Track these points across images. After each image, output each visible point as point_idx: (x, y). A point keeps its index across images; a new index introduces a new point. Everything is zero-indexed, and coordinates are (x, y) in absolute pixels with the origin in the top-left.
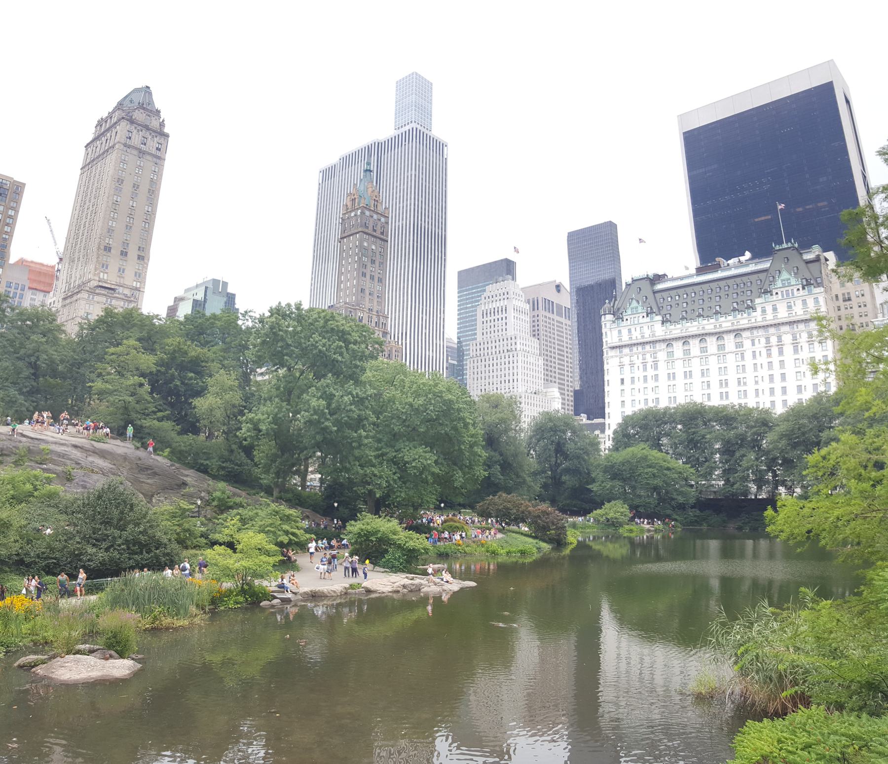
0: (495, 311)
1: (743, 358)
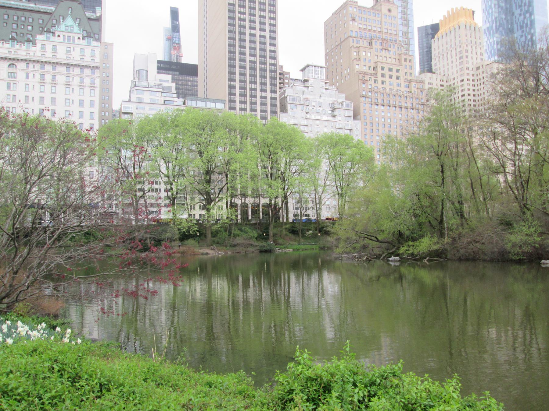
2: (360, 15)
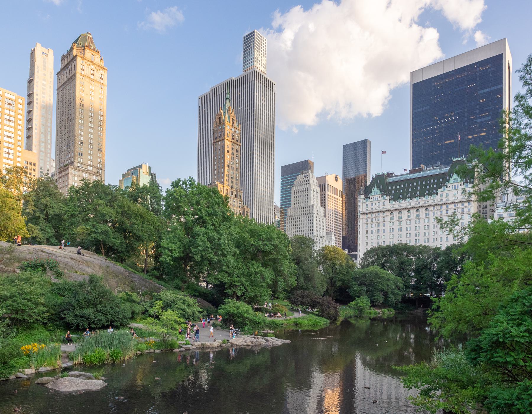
0: (301, 191)
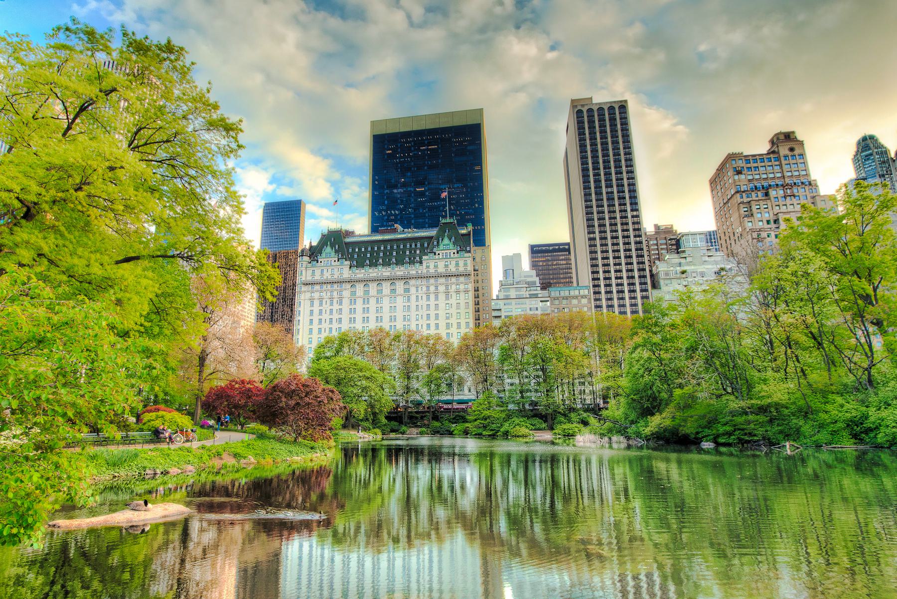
1: (409, 300)
2: (749, 165)
